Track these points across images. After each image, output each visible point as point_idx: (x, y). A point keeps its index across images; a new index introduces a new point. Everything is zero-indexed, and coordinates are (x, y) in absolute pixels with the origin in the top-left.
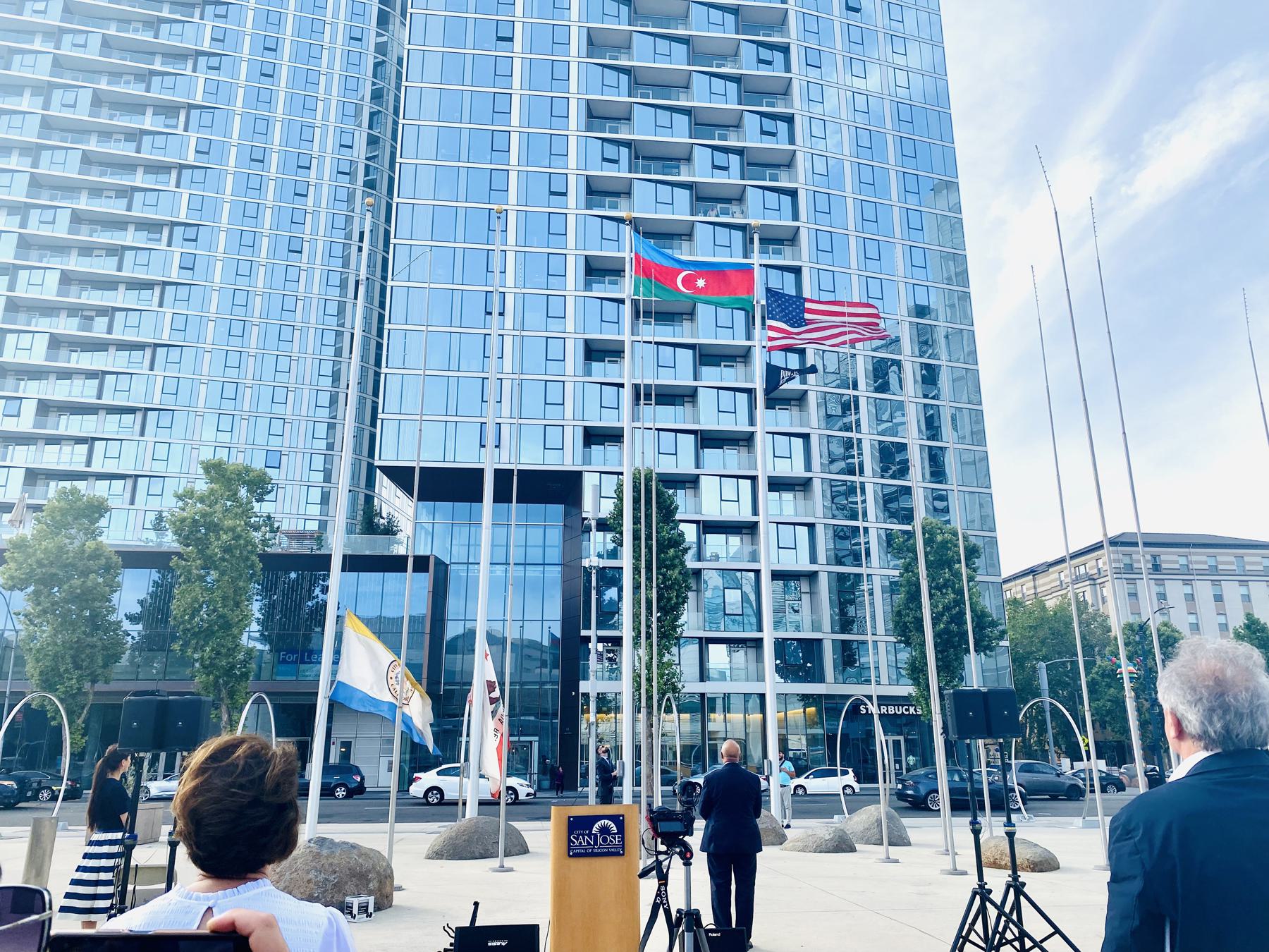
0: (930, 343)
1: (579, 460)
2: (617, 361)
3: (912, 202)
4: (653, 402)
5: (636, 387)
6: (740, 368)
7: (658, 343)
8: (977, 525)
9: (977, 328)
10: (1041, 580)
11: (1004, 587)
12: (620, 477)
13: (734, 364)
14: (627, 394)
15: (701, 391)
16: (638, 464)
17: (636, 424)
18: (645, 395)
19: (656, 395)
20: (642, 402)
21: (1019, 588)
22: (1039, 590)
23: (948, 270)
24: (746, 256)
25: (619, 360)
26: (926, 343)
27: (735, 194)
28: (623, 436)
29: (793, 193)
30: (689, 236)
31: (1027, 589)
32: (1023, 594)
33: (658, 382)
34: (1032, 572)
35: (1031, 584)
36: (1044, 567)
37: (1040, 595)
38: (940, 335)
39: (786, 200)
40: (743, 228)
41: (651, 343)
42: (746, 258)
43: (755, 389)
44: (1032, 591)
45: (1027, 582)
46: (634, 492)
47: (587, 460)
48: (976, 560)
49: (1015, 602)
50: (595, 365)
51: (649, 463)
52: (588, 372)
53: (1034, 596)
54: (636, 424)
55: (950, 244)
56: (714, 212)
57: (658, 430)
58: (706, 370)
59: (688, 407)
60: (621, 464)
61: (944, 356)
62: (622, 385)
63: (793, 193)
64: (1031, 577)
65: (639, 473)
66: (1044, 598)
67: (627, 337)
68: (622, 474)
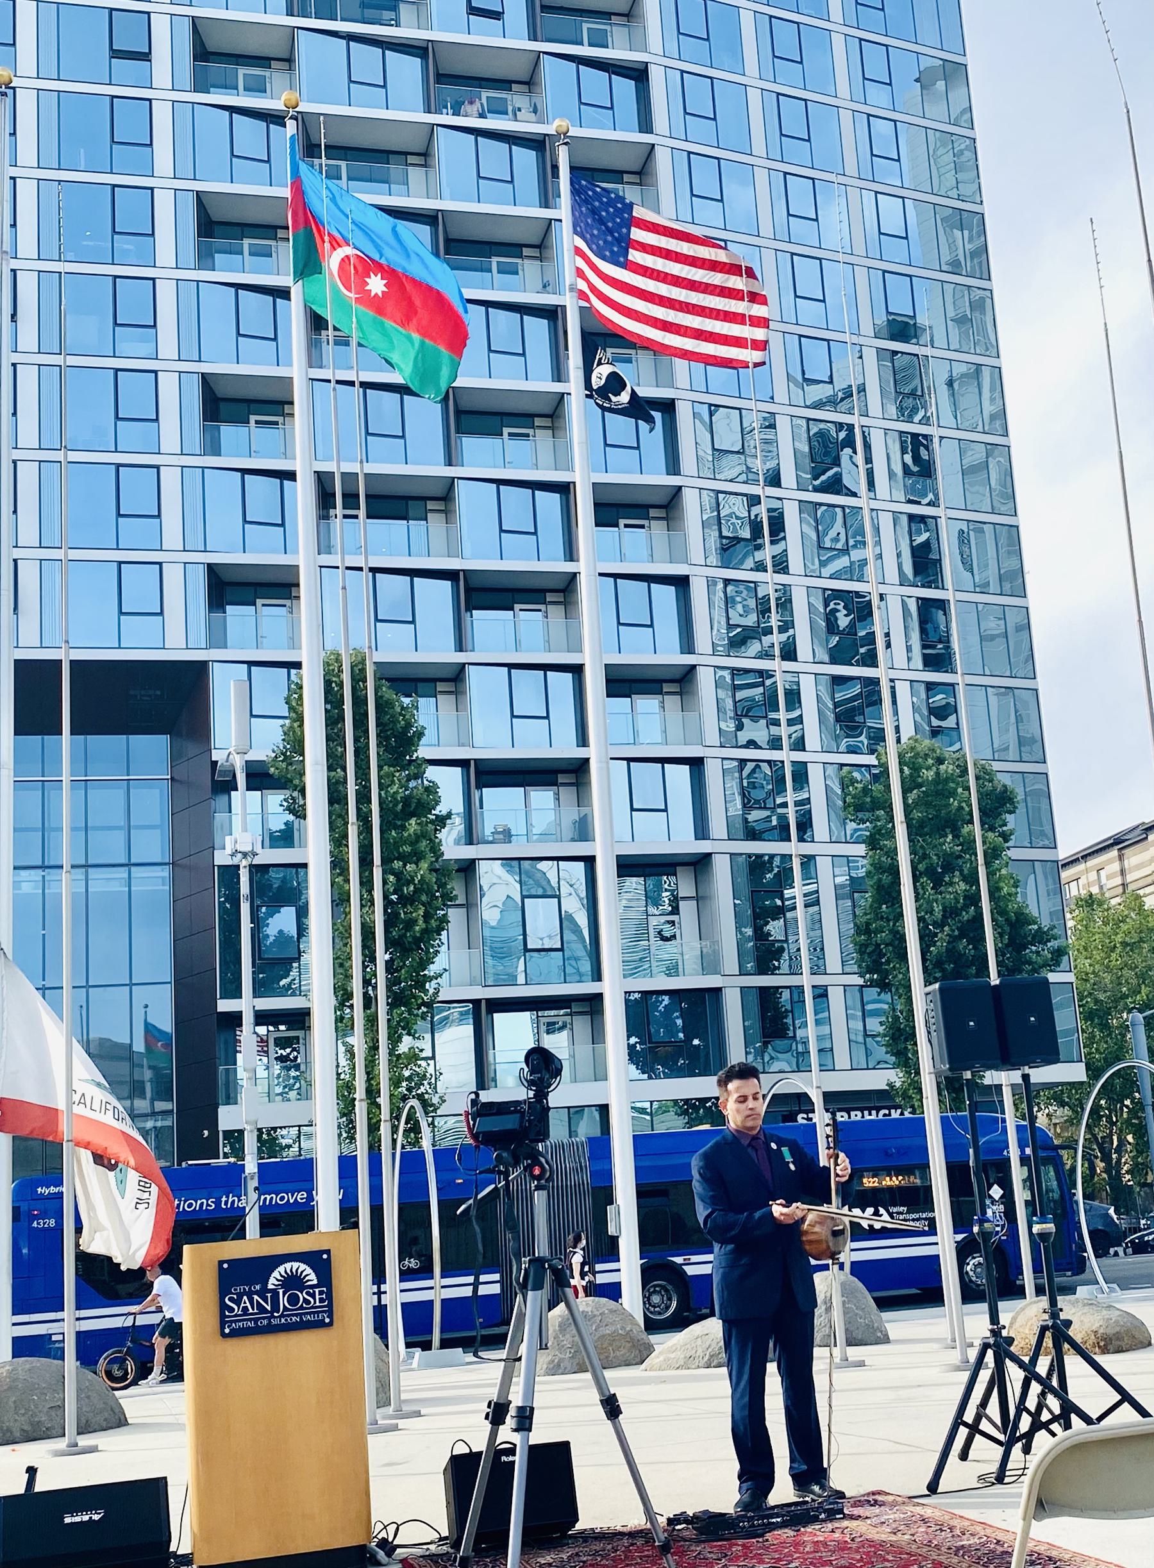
0: (919, 393)
1: (199, 633)
2: (277, 423)
3: (878, 97)
4: (362, 512)
5: (323, 481)
6: (543, 438)
7: (365, 385)
8: (1013, 754)
9: (1005, 362)
10: (1134, 857)
11: (1065, 875)
12: (293, 671)
13: (530, 431)
14: (303, 494)
15: (461, 488)
16: (336, 641)
17: (325, 559)
18: (344, 495)
19: (367, 496)
20: (339, 510)
21: (1093, 876)
22: (1129, 878)
23: (952, 245)
24: (546, 203)
25: (280, 419)
26: (913, 394)
27: (520, 71)
28: (298, 585)
29: (639, 74)
30: (425, 156)
31: (1109, 877)
32: (1101, 887)
33: (371, 468)
34: (1118, 842)
35: (1116, 866)
36: (1138, 831)
37: (1131, 887)
38: (937, 374)
39: (625, 87)
40: (538, 144)
41: (352, 383)
42: (547, 207)
43: (574, 483)
44: (1118, 880)
45: (1110, 861)
46: (326, 702)
47: (217, 638)
48: (1009, 818)
49: (1089, 902)
50: (227, 432)
51: (361, 640)
52: (213, 447)
53: (1120, 890)
54: (325, 559)
55: (954, 194)
56: (475, 108)
57: (375, 570)
58: (470, 444)
59: (436, 522)
60: (294, 644)
61: (947, 419)
62: (291, 476)
63: (639, 74)
64: (1114, 853)
65: (338, 660)
66: (1141, 892)
67: (296, 370)
68: (298, 665)
